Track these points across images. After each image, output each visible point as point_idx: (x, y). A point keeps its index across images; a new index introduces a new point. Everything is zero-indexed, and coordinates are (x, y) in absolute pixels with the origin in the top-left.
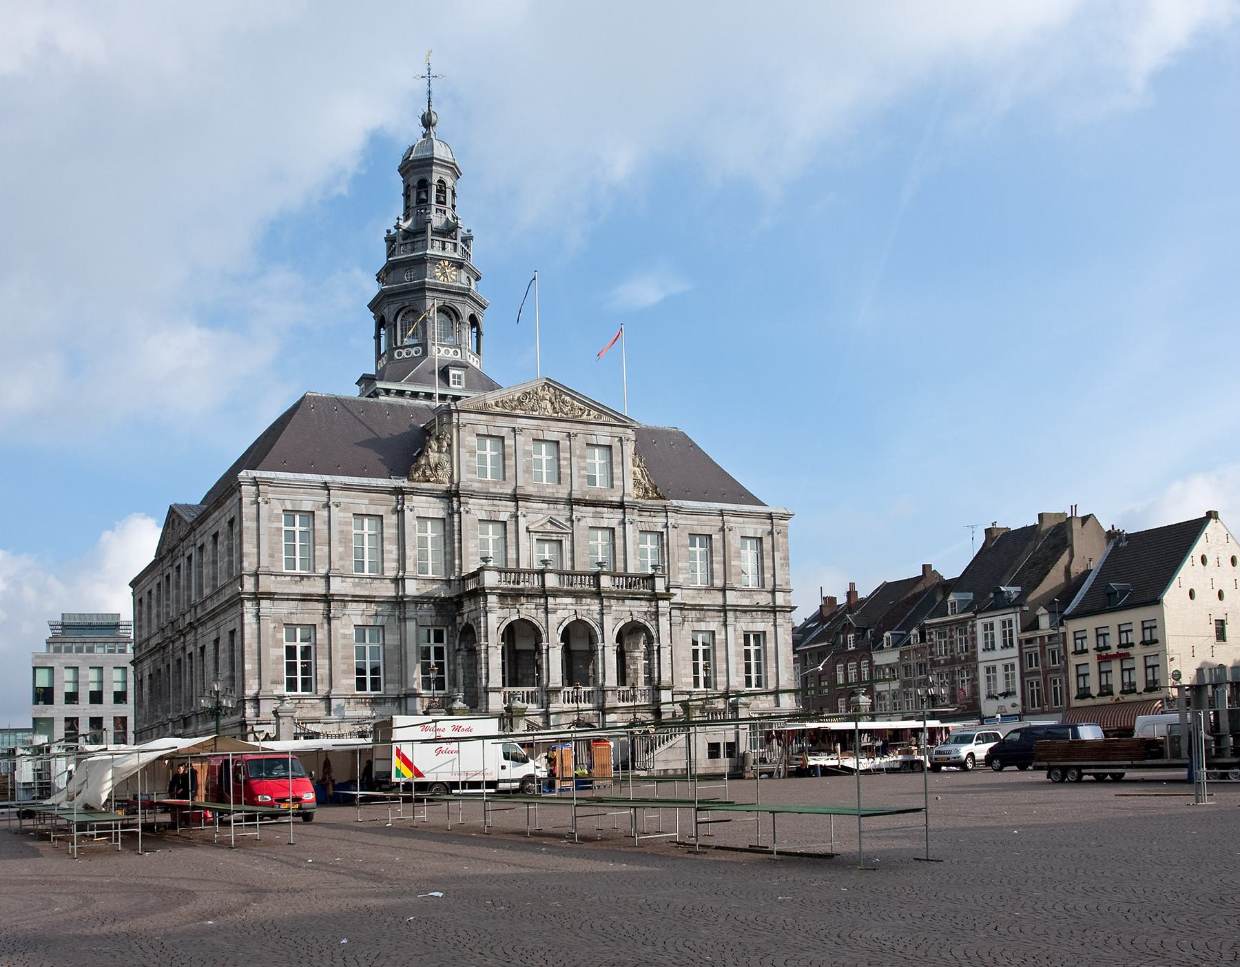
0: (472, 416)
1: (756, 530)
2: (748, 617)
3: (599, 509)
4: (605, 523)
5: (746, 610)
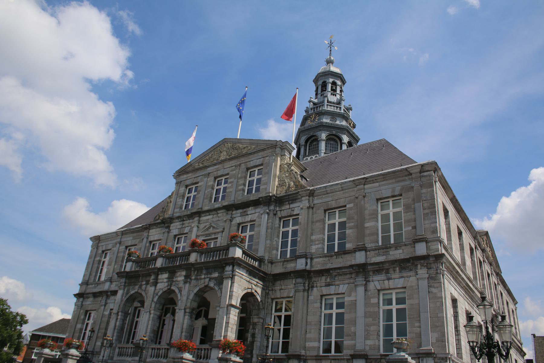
0: (185, 176)
1: (393, 191)
2: (383, 277)
3: (244, 210)
4: (248, 218)
5: (380, 268)
